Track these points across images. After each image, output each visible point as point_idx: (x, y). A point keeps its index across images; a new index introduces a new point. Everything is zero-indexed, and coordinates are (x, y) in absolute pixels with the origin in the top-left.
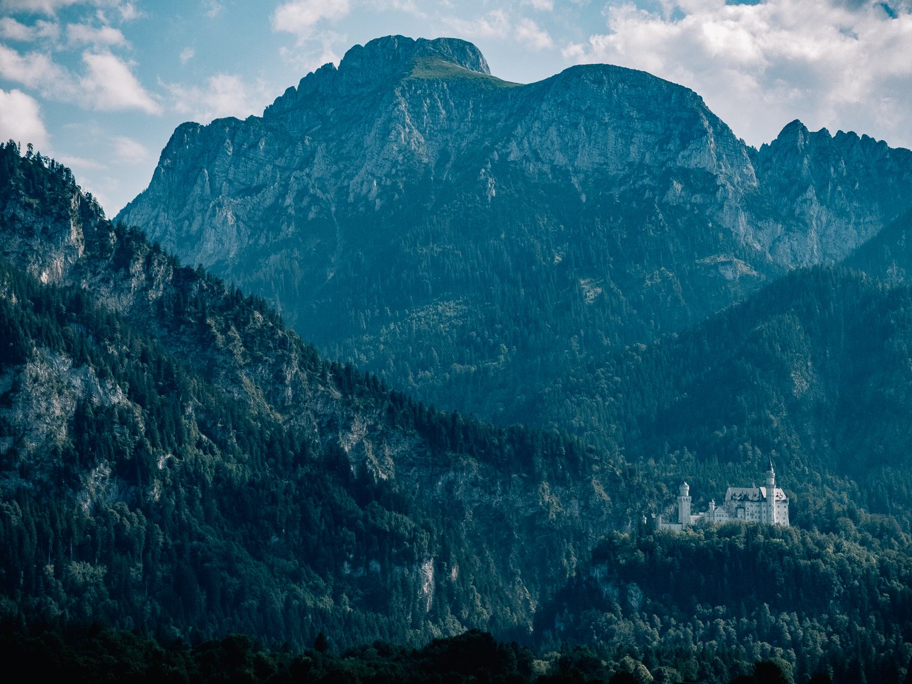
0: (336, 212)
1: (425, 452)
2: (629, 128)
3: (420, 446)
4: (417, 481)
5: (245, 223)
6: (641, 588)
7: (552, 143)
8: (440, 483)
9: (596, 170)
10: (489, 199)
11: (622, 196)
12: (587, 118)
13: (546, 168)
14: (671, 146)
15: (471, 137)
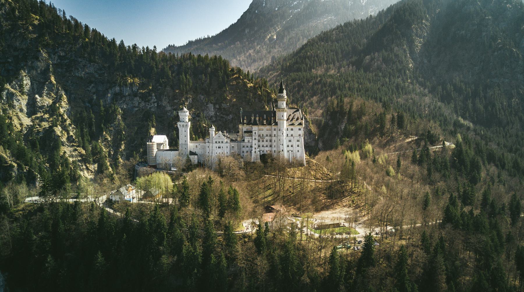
1: (104, 73)
3: (101, 70)
8: (109, 95)
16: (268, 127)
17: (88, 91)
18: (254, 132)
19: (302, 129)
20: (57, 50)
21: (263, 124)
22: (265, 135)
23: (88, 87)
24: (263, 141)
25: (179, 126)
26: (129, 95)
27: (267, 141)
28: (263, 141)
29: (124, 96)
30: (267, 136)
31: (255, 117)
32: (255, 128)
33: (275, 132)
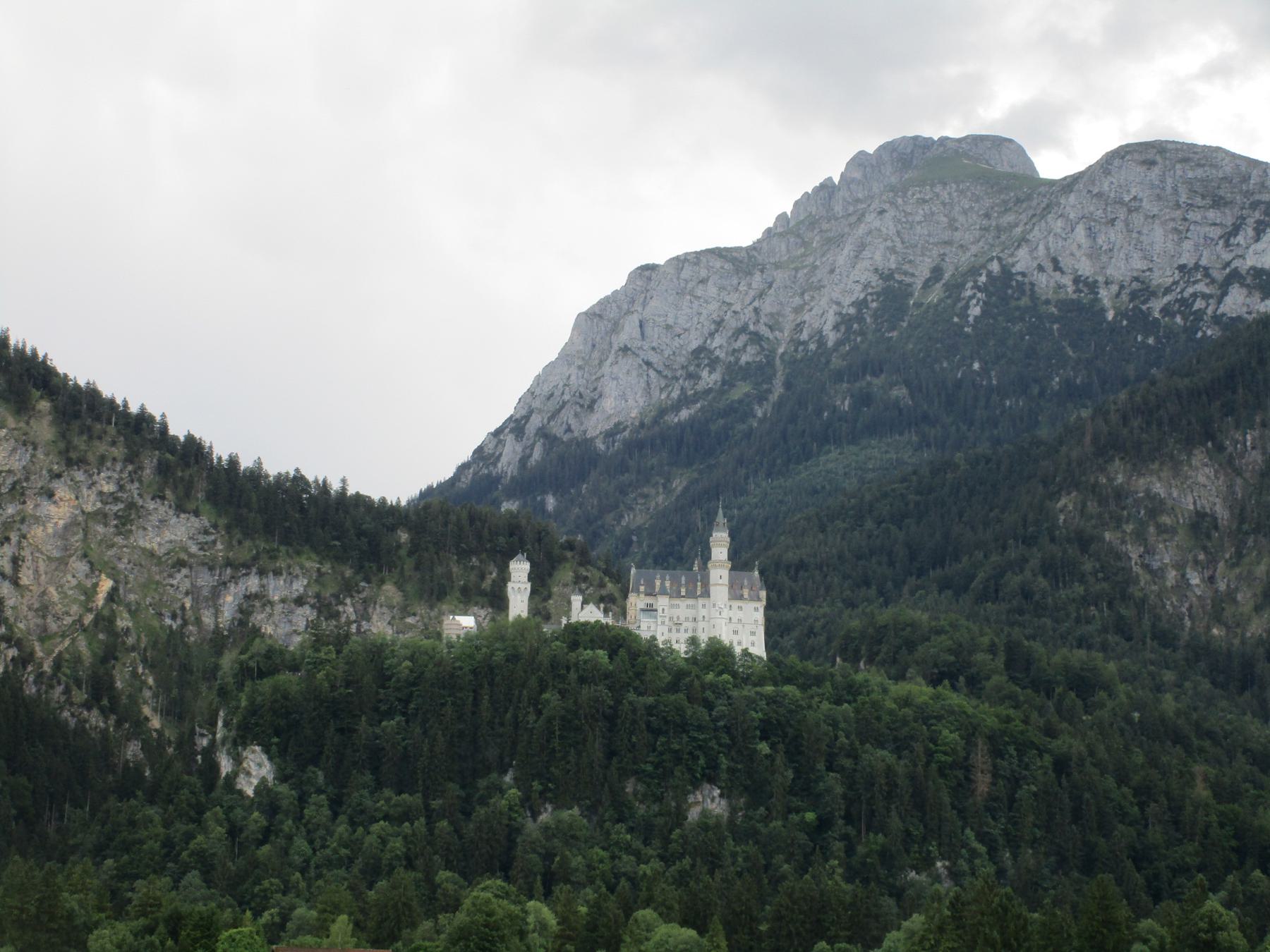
0: (783, 354)
1: (214, 542)
2: (1185, 219)
3: (206, 532)
4: (187, 594)
5: (659, 372)
6: (270, 759)
7: (1079, 246)
8: (229, 599)
9: (1136, 279)
10: (971, 319)
11: (1165, 311)
12: (1130, 211)
13: (1067, 281)
14: (1240, 239)
15: (974, 249)
16: (690, 602)
17: (172, 586)
18: (660, 611)
19: (762, 610)
20: (95, 477)
21: (679, 596)
22: (682, 618)
23: (171, 576)
24: (678, 631)
25: (509, 589)
26: (283, 601)
27: (686, 631)
28: (678, 631)
29: (269, 602)
30: (687, 619)
31: (663, 579)
32: (662, 602)
33: (703, 612)
